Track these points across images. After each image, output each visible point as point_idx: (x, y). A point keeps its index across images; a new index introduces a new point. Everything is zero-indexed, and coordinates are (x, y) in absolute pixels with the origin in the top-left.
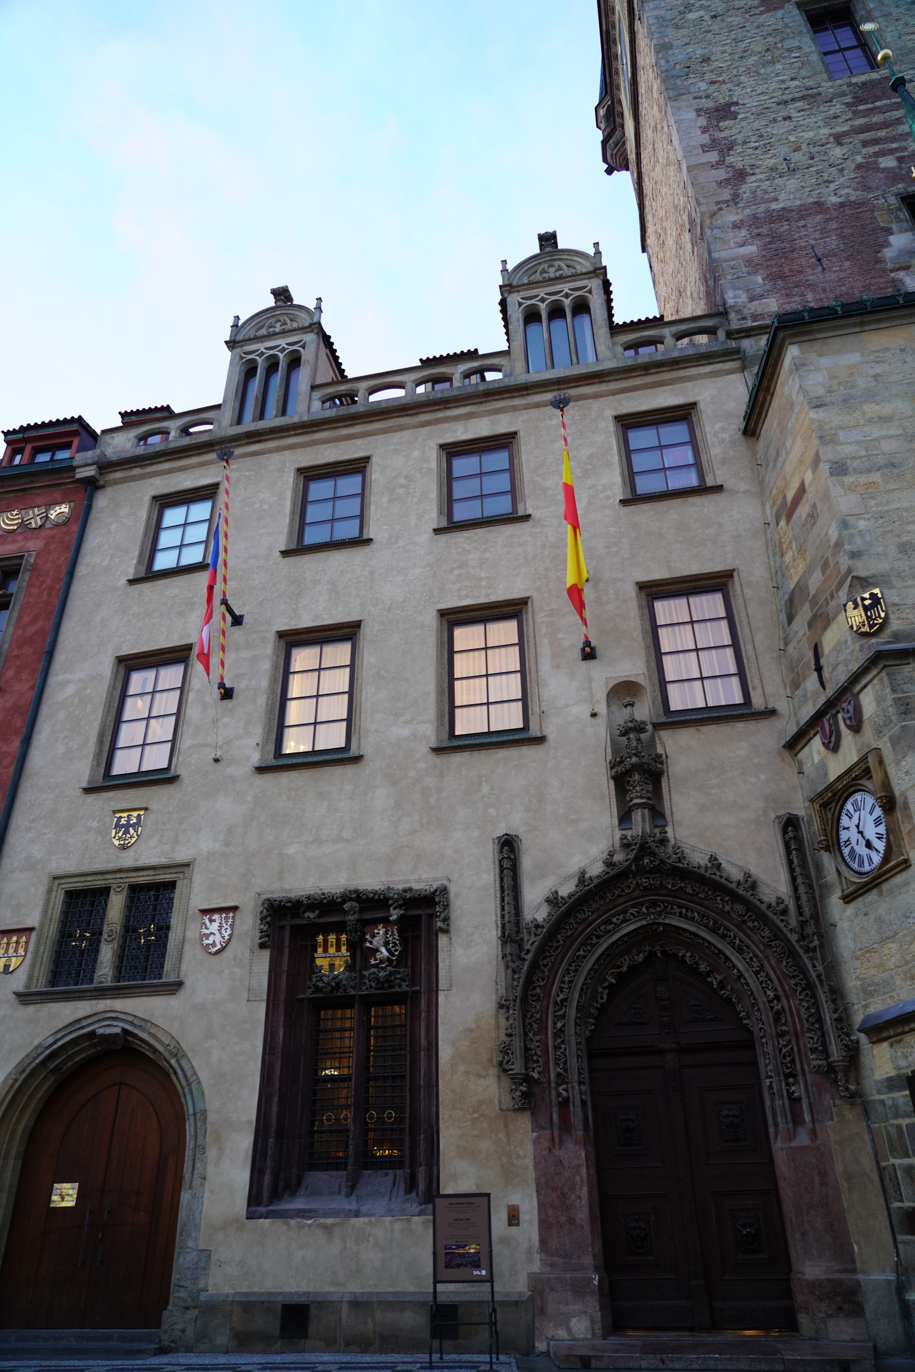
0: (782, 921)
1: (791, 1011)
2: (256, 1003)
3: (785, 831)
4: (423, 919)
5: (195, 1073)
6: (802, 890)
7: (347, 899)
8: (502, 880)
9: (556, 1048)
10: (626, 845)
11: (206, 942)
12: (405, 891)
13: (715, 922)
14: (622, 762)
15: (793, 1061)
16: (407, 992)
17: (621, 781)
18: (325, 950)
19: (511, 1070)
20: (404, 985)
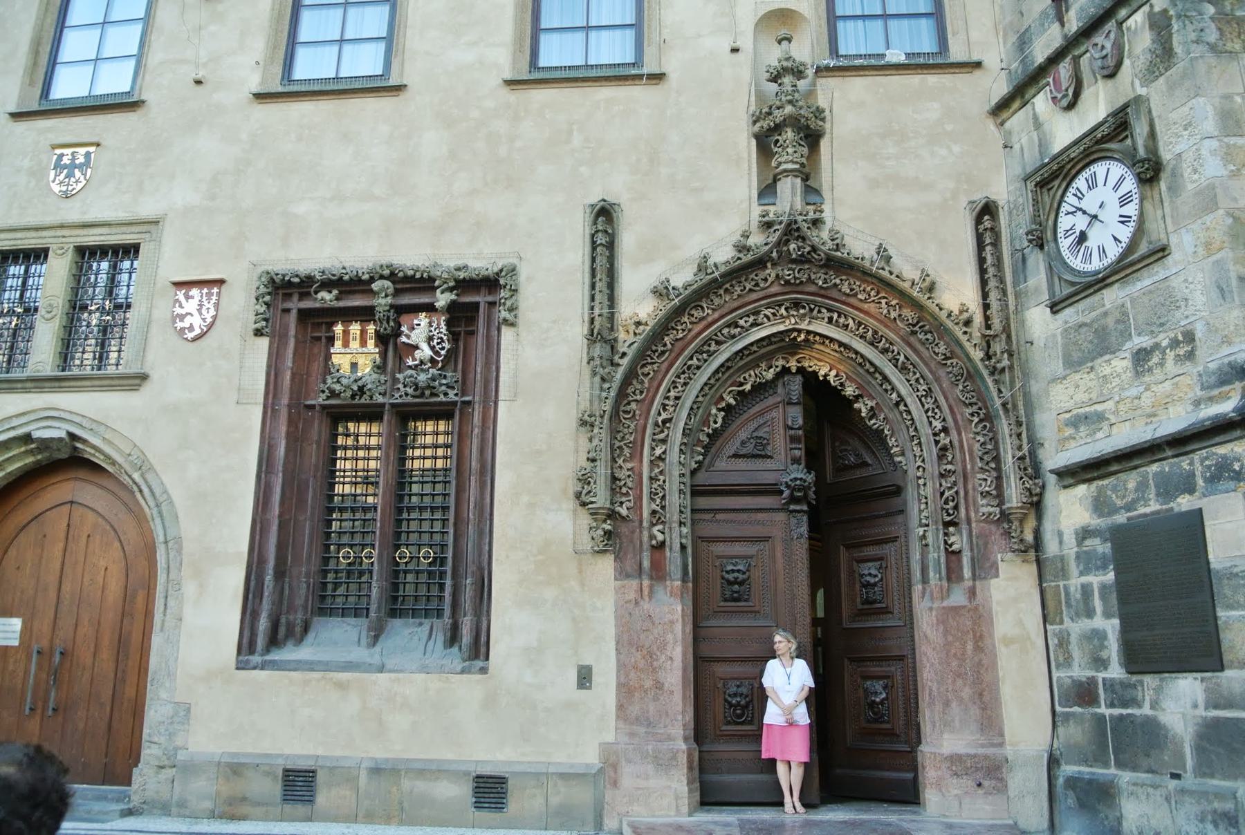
0: (965, 333)
1: (962, 446)
2: (248, 407)
3: (978, 220)
4: (481, 310)
5: (165, 492)
6: (993, 297)
7: (377, 277)
8: (593, 260)
9: (651, 479)
10: (767, 225)
11: (179, 325)
12: (458, 269)
13: (875, 332)
14: (769, 114)
15: (956, 507)
16: (454, 403)
17: (765, 142)
18: (346, 344)
19: (592, 503)
20: (451, 393)
